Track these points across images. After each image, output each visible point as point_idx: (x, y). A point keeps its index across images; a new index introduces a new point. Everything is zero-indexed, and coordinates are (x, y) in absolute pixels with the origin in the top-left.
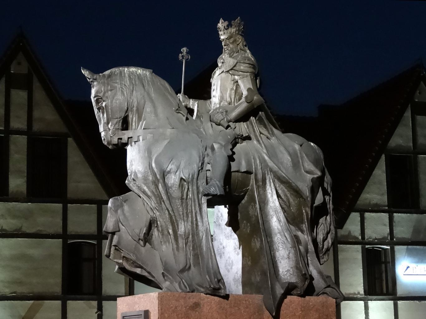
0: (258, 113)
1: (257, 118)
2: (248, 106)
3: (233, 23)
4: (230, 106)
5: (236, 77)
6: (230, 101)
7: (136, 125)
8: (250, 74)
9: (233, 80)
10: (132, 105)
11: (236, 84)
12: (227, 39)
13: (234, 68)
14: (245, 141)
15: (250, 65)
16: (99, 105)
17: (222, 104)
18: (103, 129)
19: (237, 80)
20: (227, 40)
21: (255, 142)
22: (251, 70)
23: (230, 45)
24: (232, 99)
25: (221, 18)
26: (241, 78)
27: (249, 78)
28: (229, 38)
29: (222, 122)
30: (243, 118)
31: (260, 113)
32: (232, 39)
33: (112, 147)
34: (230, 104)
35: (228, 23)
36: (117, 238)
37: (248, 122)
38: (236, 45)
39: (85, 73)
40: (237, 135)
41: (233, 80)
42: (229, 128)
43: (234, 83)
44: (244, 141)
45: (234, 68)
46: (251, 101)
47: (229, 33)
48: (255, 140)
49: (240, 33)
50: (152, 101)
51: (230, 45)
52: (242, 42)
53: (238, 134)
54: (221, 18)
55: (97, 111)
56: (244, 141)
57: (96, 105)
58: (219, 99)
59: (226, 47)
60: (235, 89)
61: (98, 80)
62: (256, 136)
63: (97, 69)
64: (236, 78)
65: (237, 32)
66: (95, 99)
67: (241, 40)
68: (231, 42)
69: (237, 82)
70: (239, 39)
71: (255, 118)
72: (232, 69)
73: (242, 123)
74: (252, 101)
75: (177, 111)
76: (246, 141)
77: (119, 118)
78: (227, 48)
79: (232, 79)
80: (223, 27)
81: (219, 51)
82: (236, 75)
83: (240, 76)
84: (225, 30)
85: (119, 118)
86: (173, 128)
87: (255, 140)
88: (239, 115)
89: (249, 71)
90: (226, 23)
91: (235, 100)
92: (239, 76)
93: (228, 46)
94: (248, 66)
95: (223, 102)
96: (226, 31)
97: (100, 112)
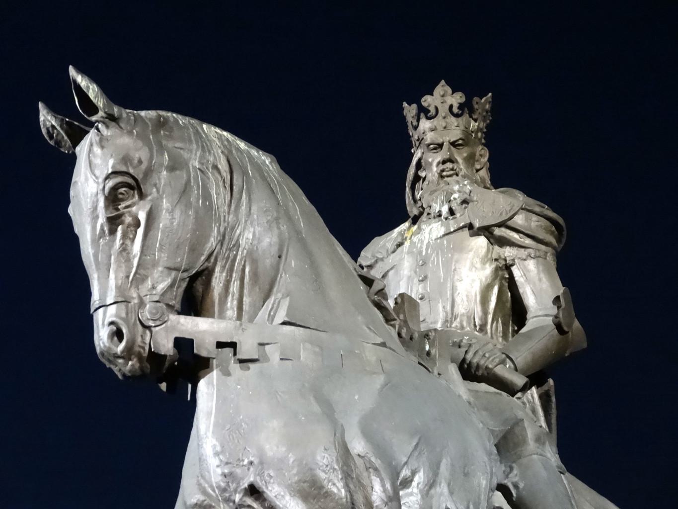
5: (508, 252)
10: (231, 239)
11: (500, 273)
13: (510, 223)
16: (118, 210)
17: (454, 325)
18: (116, 297)
19: (513, 260)
25: (443, 82)
28: (460, 142)
33: (137, 365)
35: (463, 100)
39: (88, 87)
41: (496, 260)
43: (497, 269)
50: (302, 241)
54: (443, 82)
55: (102, 229)
57: (107, 207)
61: (122, 125)
63: (128, 94)
66: (110, 184)
69: (508, 267)
72: (500, 225)
75: (376, 298)
78: (452, 169)
79: (494, 257)
84: (453, 119)
85: (184, 271)
86: (383, 345)
91: (495, 322)
97: (113, 232)
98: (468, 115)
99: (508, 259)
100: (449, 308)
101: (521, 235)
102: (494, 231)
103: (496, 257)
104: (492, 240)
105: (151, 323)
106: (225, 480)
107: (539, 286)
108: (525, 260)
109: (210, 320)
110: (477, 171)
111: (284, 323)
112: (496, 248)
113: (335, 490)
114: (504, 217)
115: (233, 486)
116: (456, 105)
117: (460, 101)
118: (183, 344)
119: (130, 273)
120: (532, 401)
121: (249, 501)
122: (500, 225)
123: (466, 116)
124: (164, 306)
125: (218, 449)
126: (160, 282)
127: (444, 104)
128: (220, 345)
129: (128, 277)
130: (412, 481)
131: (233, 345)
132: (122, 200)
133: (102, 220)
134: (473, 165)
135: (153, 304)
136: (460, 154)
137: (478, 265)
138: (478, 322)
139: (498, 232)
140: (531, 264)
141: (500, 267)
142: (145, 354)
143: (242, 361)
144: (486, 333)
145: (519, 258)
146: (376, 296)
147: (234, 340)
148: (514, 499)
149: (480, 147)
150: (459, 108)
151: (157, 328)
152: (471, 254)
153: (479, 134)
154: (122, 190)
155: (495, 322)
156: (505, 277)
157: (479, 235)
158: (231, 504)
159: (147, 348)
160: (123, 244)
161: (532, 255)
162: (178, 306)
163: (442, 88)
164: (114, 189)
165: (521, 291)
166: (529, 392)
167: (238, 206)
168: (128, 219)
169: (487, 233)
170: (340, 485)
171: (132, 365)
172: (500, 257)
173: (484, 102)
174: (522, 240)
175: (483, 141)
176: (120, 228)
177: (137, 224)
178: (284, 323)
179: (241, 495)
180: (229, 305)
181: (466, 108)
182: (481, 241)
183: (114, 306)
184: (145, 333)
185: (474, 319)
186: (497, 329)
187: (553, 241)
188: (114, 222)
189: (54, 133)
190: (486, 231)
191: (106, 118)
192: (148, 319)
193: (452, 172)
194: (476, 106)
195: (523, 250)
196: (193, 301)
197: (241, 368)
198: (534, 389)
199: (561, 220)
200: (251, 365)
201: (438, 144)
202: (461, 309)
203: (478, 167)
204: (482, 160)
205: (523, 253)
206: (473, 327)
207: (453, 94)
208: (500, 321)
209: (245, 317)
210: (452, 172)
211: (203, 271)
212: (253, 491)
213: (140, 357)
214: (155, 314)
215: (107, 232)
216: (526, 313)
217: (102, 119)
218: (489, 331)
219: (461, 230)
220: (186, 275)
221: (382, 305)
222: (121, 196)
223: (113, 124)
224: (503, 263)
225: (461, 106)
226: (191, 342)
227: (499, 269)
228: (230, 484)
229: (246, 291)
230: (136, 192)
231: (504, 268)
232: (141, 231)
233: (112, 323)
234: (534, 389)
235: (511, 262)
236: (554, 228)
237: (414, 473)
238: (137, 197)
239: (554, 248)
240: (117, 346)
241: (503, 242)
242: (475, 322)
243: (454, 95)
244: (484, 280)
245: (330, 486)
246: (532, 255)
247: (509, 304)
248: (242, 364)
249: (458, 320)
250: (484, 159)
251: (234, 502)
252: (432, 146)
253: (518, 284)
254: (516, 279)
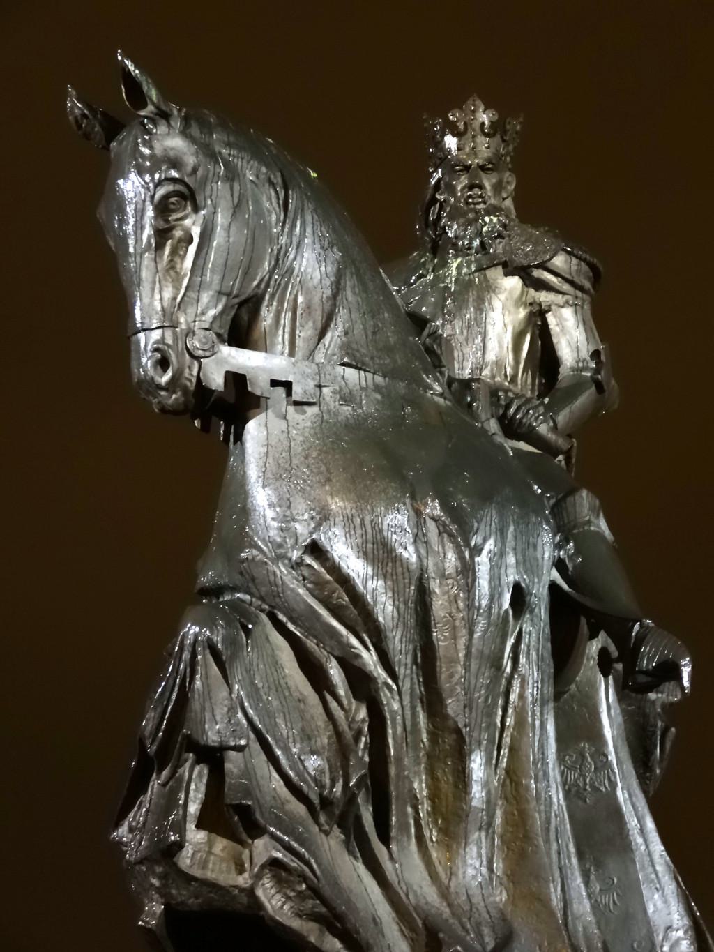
5: (544, 297)
11: (533, 319)
13: (548, 265)
16: (167, 221)
19: (550, 306)
33: (182, 399)
34: (513, 380)
35: (496, 118)
41: (531, 304)
43: (531, 316)
57: (155, 218)
66: (161, 192)
77: (237, 296)
78: (480, 196)
79: (528, 302)
83: (566, 297)
97: (160, 247)
99: (543, 304)
101: (560, 279)
102: (532, 272)
103: (531, 301)
104: (528, 282)
105: (200, 353)
106: (282, 534)
107: (572, 337)
108: (562, 307)
109: (263, 354)
110: (504, 199)
112: (532, 291)
113: (405, 554)
115: (290, 542)
118: (237, 380)
119: (178, 294)
121: (308, 560)
122: (537, 266)
123: (498, 138)
124: (215, 336)
125: (274, 500)
126: (208, 309)
128: (274, 383)
129: (175, 299)
130: (482, 549)
131: (287, 386)
132: (174, 211)
133: (148, 231)
134: (500, 193)
135: (203, 332)
136: (489, 180)
137: (512, 309)
138: (509, 371)
140: (568, 313)
142: (192, 386)
143: (296, 403)
144: (517, 385)
145: (556, 305)
147: (290, 379)
148: (570, 573)
149: (508, 174)
151: (207, 360)
152: (502, 297)
153: (508, 159)
154: (173, 200)
155: (524, 376)
156: (537, 325)
157: (513, 274)
158: (286, 561)
159: (194, 380)
160: (171, 261)
161: (571, 302)
162: (226, 336)
164: (166, 197)
165: (555, 341)
167: (293, 226)
168: (178, 233)
169: (522, 274)
170: (411, 549)
171: (176, 399)
172: (535, 301)
173: (515, 125)
174: (560, 284)
175: (510, 166)
176: (169, 242)
177: (190, 240)
179: (301, 552)
181: (496, 129)
182: (514, 283)
183: (160, 330)
184: (192, 363)
185: (505, 369)
186: (526, 380)
187: (588, 285)
188: (162, 235)
189: (82, 123)
191: (157, 114)
192: (198, 349)
194: (508, 127)
195: (561, 296)
196: (240, 329)
197: (296, 411)
200: (306, 408)
202: (491, 356)
203: (505, 195)
204: (509, 188)
205: (560, 299)
206: (503, 377)
208: (530, 373)
209: (299, 353)
211: (253, 296)
212: (315, 549)
213: (185, 390)
214: (205, 344)
215: (154, 245)
216: (559, 367)
217: (152, 115)
218: (519, 382)
220: (237, 300)
222: (172, 207)
223: (164, 122)
224: (537, 308)
225: (492, 124)
226: (243, 377)
228: (288, 540)
230: (188, 203)
232: (192, 249)
233: (156, 350)
235: (547, 309)
236: (591, 274)
237: (485, 540)
238: (189, 208)
239: (591, 296)
240: (161, 377)
241: (541, 285)
242: (506, 372)
244: (517, 325)
245: (400, 550)
246: (571, 302)
247: (539, 354)
248: (297, 407)
249: (489, 367)
251: (290, 559)
253: (552, 333)
254: (551, 327)
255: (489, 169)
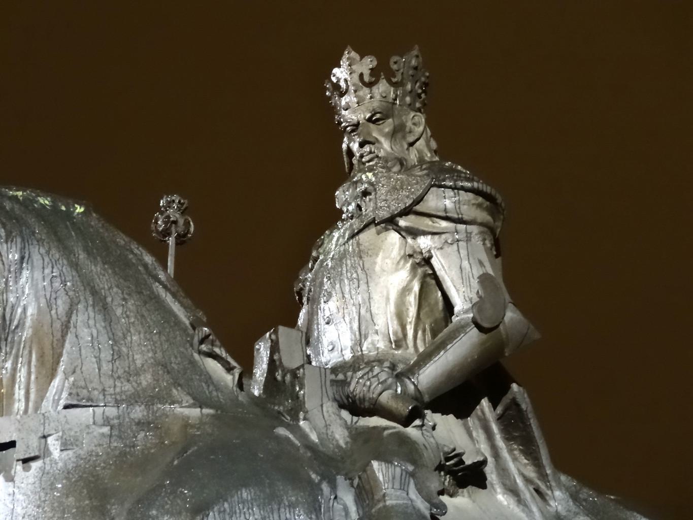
0: (508, 388)
1: (499, 409)
2: (482, 343)
3: (395, 63)
4: (400, 352)
5: (424, 242)
6: (400, 335)
7: (32, 396)
8: (482, 229)
9: (410, 256)
10: (11, 321)
12: (370, 120)
13: (418, 208)
14: (465, 490)
15: (480, 199)
19: (429, 251)
20: (371, 125)
21: (502, 498)
22: (483, 216)
23: (382, 140)
24: (408, 327)
26: (446, 242)
27: (476, 240)
28: (378, 116)
29: (386, 398)
30: (456, 398)
31: (514, 386)
32: (390, 120)
34: (399, 343)
35: (375, 63)
36: (477, 422)
37: (469, 418)
38: (406, 146)
40: (445, 453)
41: (410, 256)
42: (418, 422)
43: (415, 267)
44: (460, 490)
45: (418, 208)
46: (496, 325)
47: (378, 97)
48: (499, 490)
49: (418, 105)
51: (382, 140)
52: (424, 135)
53: (446, 449)
56: (460, 488)
58: (351, 328)
59: (367, 148)
60: (416, 287)
62: (503, 471)
64: (422, 246)
65: (408, 99)
67: (421, 128)
68: (387, 130)
69: (427, 261)
70: (414, 124)
71: (495, 407)
73: (451, 416)
74: (497, 326)
75: (204, 347)
76: (469, 487)
78: (371, 152)
79: (409, 251)
80: (356, 77)
81: (340, 170)
82: (425, 233)
83: (444, 236)
87: (499, 490)
88: (449, 376)
89: (479, 220)
90: (368, 64)
92: (436, 237)
93: (376, 144)
94: (473, 202)
95: (369, 340)
96: (365, 92)
98: (384, 81)
100: (355, 326)
102: (398, 222)
103: (411, 252)
110: (411, 144)
111: (66, 407)
114: (409, 202)
116: (366, 73)
117: (371, 66)
120: (483, 417)
127: (353, 75)
139: (402, 223)
141: (417, 264)
146: (203, 346)
147: (13, 439)
150: (371, 75)
161: (449, 241)
163: (349, 54)
166: (478, 407)
172: (415, 252)
178: (66, 407)
180: (16, 396)
190: (391, 222)
193: (371, 156)
194: (395, 67)
198: (485, 403)
199: (487, 189)
201: (353, 125)
203: (411, 139)
207: (361, 60)
210: (371, 156)
219: (367, 229)
221: (214, 354)
224: (420, 257)
227: (417, 266)
229: (33, 377)
231: (423, 263)
234: (485, 403)
241: (414, 233)
243: (364, 60)
250: (419, 127)
252: (349, 128)
255: (378, 120)
